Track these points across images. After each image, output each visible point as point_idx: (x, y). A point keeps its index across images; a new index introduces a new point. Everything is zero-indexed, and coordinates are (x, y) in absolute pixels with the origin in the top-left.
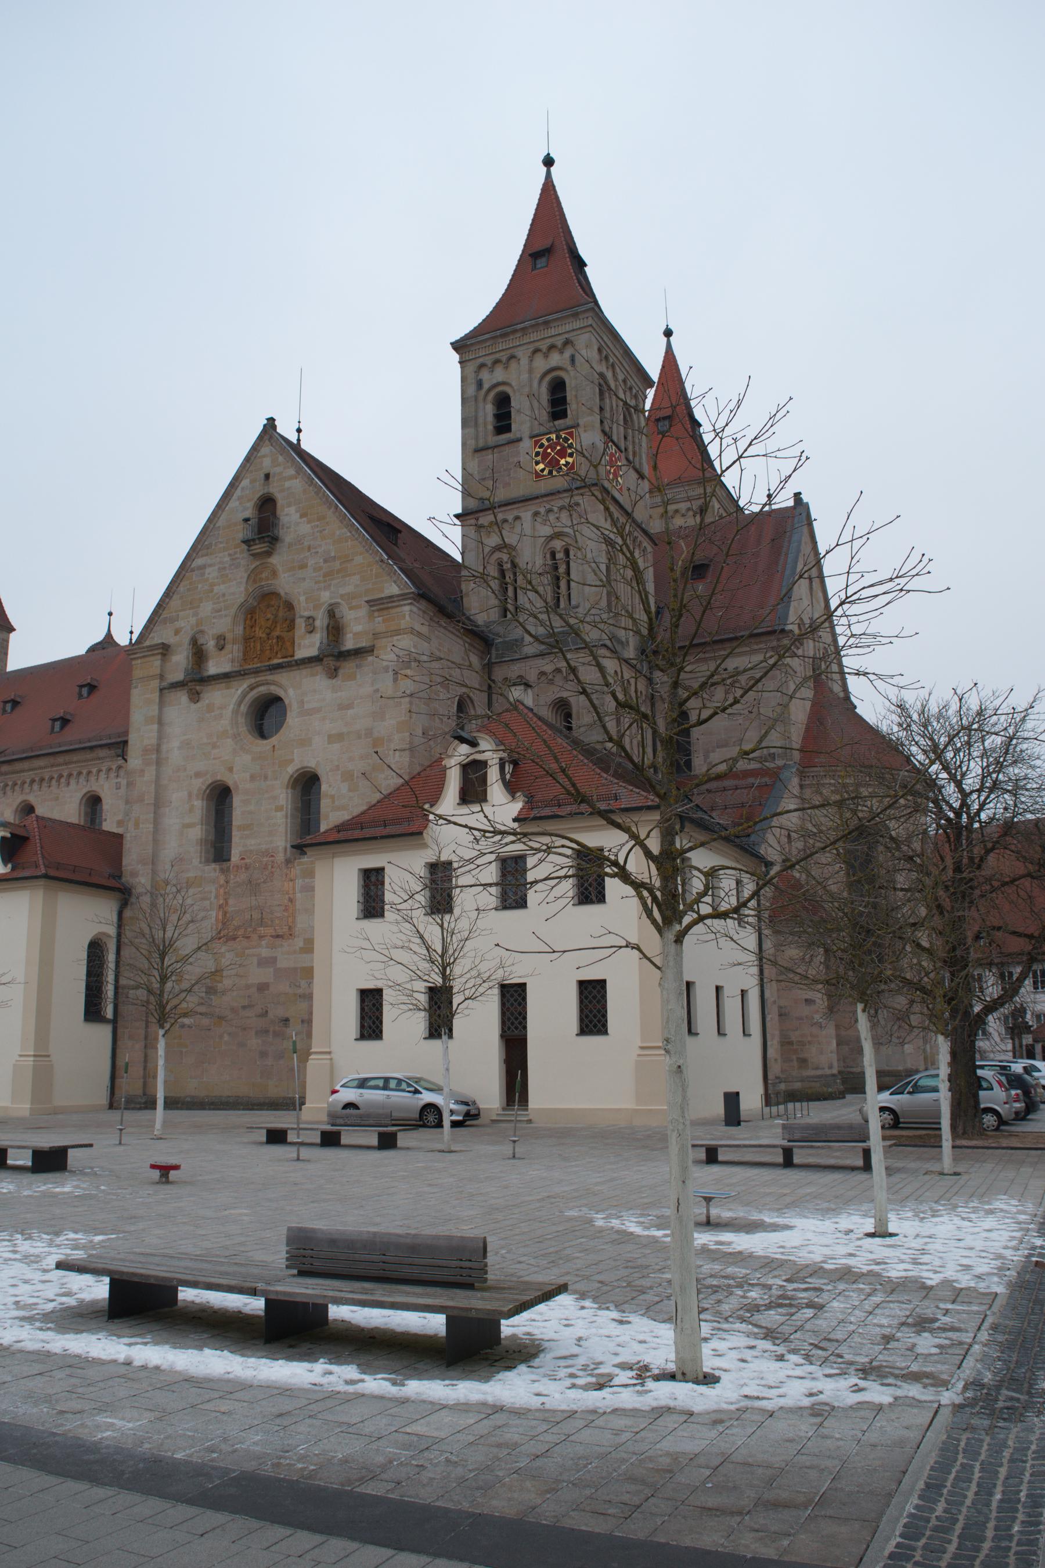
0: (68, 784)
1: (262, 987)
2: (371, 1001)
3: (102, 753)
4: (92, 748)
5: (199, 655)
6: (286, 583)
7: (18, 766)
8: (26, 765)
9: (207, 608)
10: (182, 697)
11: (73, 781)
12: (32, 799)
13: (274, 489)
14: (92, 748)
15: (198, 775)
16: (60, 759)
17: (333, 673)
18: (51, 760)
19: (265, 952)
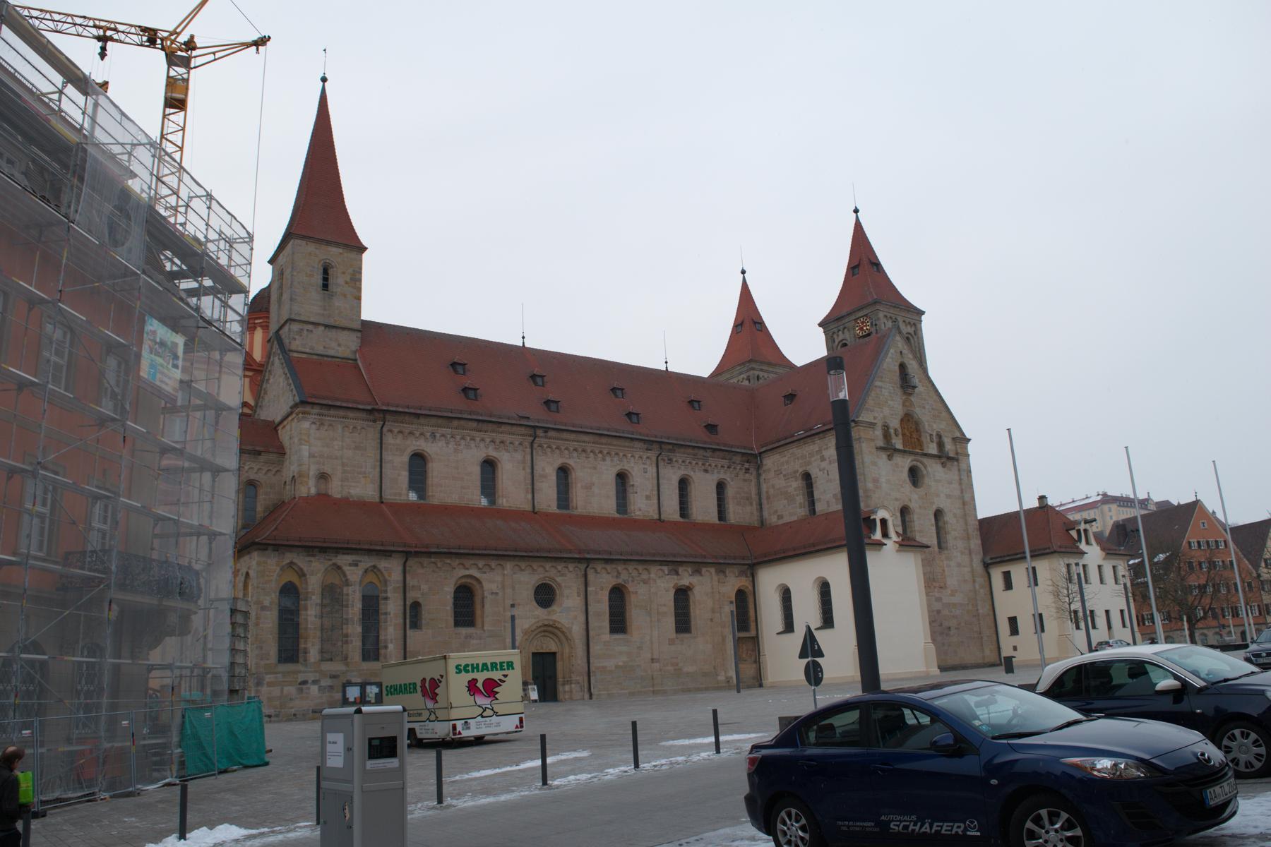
0: (604, 460)
1: (939, 612)
2: (1013, 621)
3: (637, 444)
4: (632, 439)
5: (886, 435)
6: (918, 412)
7: (565, 435)
8: (573, 436)
9: (887, 411)
10: (884, 456)
11: (608, 458)
12: (571, 462)
13: (906, 361)
14: (632, 439)
15: (897, 499)
16: (604, 440)
17: (944, 465)
18: (597, 439)
19: (937, 595)
